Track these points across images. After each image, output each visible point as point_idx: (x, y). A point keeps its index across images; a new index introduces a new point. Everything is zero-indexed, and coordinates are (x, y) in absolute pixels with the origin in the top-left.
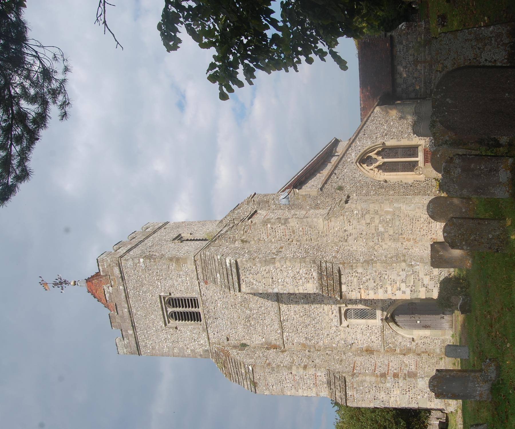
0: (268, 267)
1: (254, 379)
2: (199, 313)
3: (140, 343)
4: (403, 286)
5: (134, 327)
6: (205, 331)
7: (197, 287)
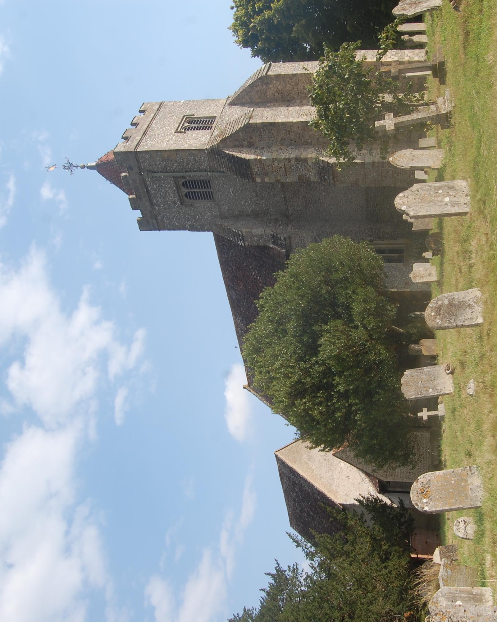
0: (293, 65)
1: (252, 114)
2: (212, 127)
3: (141, 143)
4: (393, 57)
5: (144, 134)
6: (210, 133)
7: (220, 112)
